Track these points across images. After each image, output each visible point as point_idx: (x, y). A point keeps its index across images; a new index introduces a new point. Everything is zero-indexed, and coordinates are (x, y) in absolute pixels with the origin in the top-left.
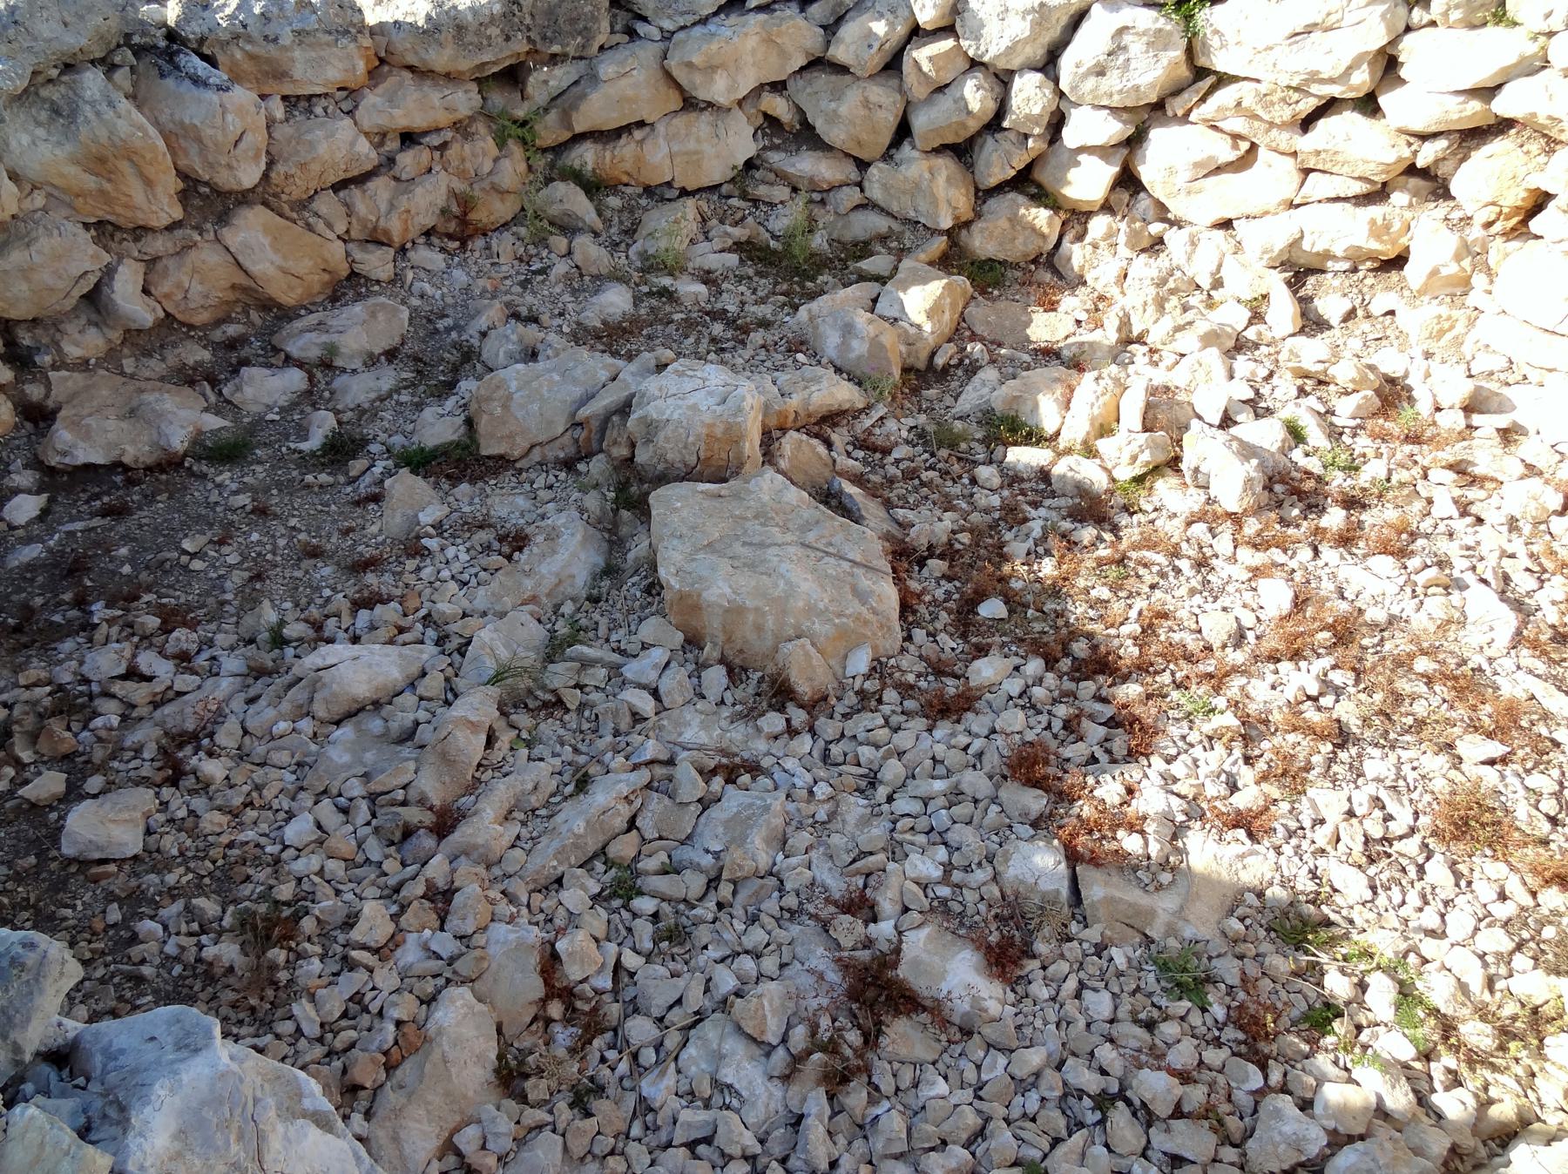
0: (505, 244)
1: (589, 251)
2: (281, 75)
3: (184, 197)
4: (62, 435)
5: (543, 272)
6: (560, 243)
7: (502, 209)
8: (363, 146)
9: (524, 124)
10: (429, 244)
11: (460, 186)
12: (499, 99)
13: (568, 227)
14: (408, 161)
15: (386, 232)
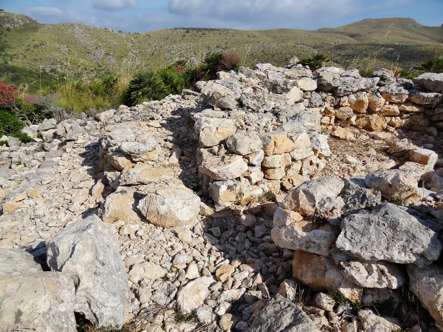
0: (414, 133)
1: (432, 139)
2: (391, 98)
3: (367, 110)
4: (335, 132)
5: (419, 139)
6: (426, 136)
7: (419, 128)
8: (398, 111)
9: (430, 116)
10: (402, 130)
11: (412, 122)
12: (427, 112)
13: (430, 134)
14: (405, 116)
15: (395, 124)
